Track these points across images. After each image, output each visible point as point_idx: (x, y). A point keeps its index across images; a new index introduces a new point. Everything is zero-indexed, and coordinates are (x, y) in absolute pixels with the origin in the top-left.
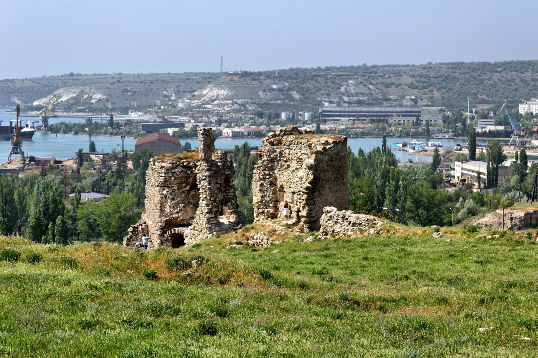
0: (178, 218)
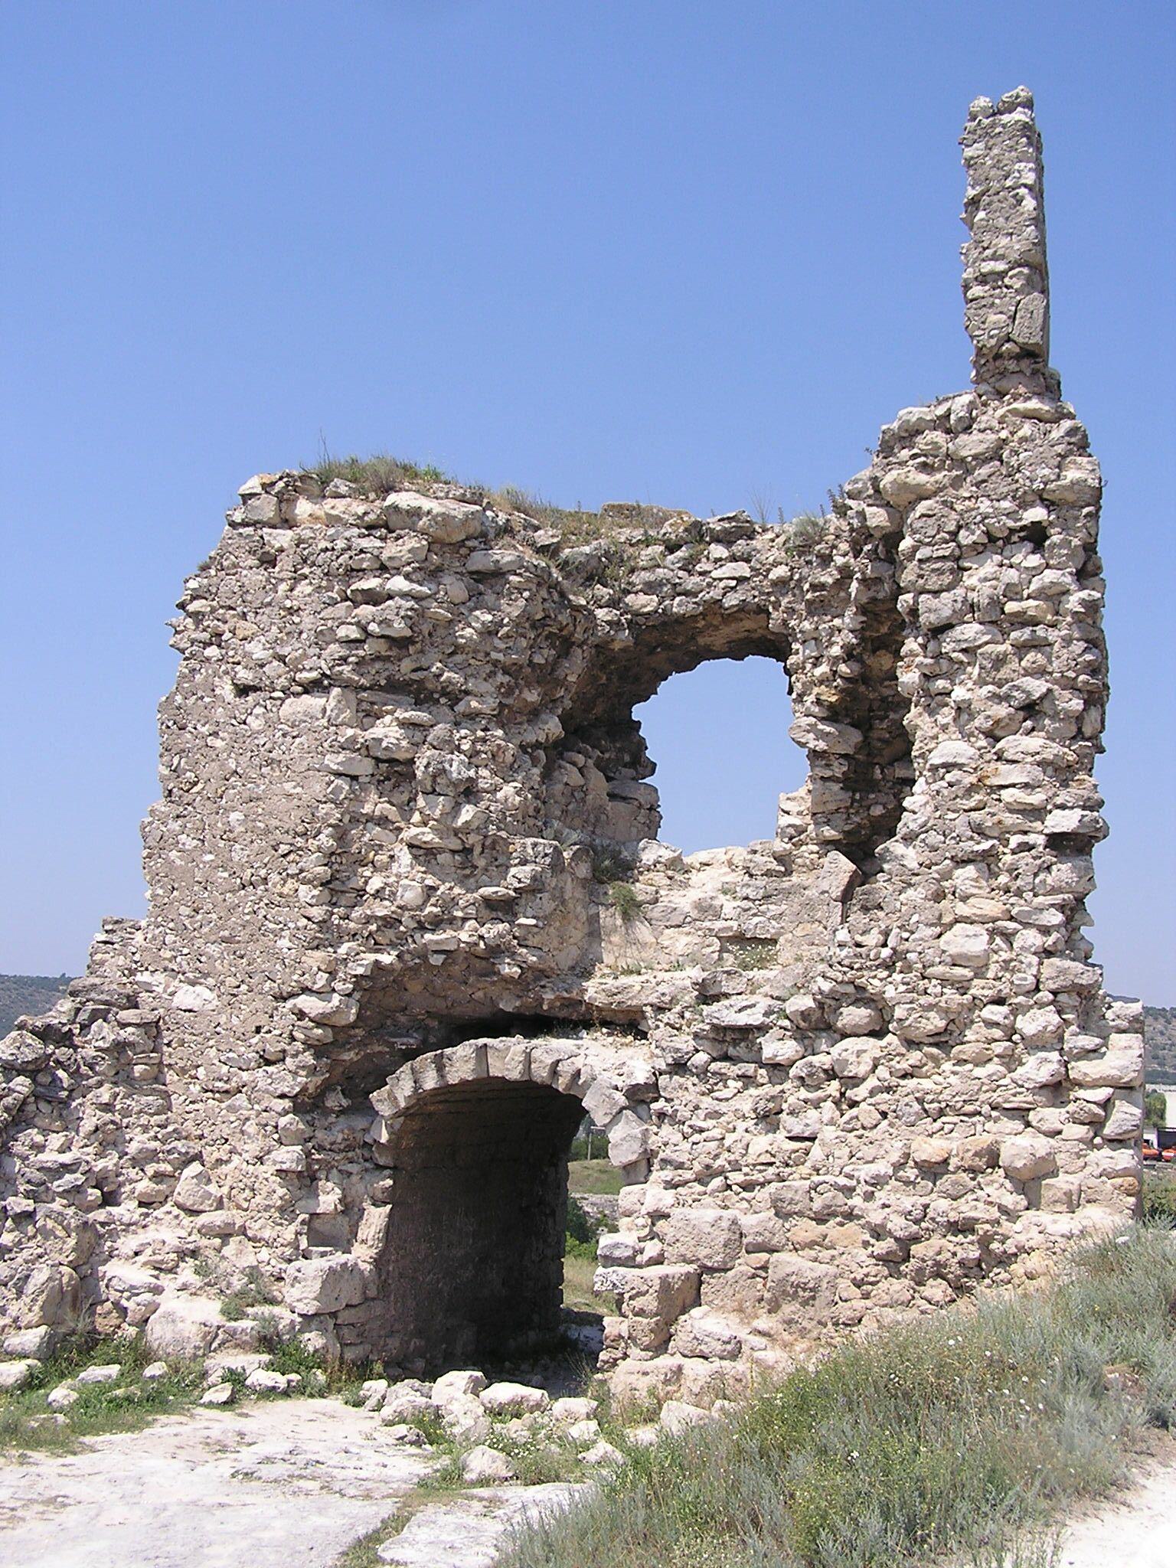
0: (496, 951)
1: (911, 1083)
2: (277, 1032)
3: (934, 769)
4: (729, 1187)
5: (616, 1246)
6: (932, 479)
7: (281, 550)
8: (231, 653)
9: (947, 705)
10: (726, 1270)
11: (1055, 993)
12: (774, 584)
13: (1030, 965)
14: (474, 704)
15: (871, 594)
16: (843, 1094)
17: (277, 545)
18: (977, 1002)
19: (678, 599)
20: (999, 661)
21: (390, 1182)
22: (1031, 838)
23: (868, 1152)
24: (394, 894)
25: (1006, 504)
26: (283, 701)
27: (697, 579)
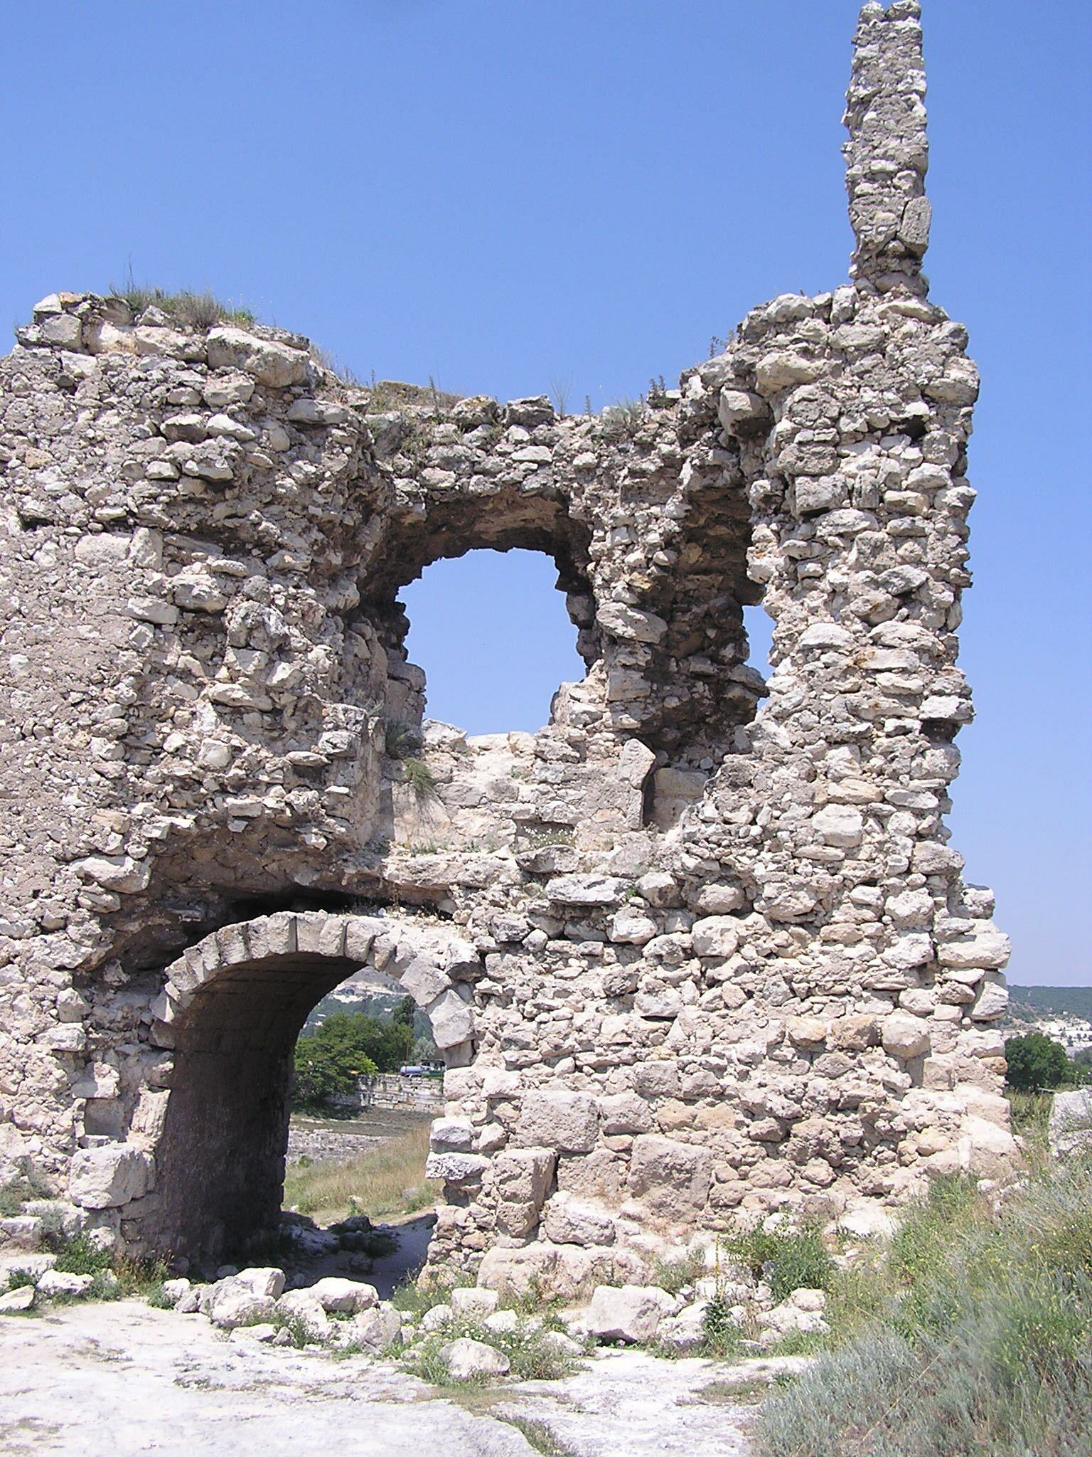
0: (303, 819)
1: (779, 963)
2: (60, 897)
3: (808, 650)
4: (578, 1068)
5: (452, 1130)
6: (813, 365)
7: (82, 377)
8: (19, 482)
9: (815, 588)
10: (586, 1153)
11: (927, 875)
12: (578, 470)
13: (904, 847)
14: (288, 559)
15: (707, 481)
16: (703, 974)
17: (77, 371)
18: (848, 883)
19: (475, 478)
20: (877, 548)
21: (169, 1065)
22: (907, 723)
23: (733, 1032)
24: (195, 752)
25: (889, 396)
26: (80, 538)
27: (497, 459)
